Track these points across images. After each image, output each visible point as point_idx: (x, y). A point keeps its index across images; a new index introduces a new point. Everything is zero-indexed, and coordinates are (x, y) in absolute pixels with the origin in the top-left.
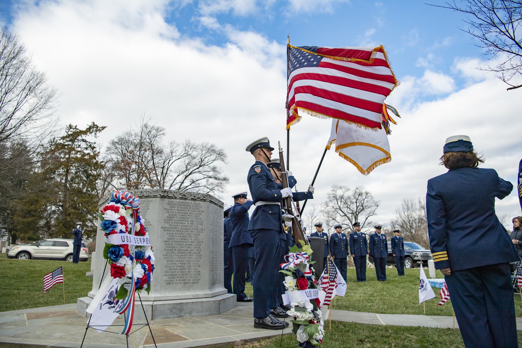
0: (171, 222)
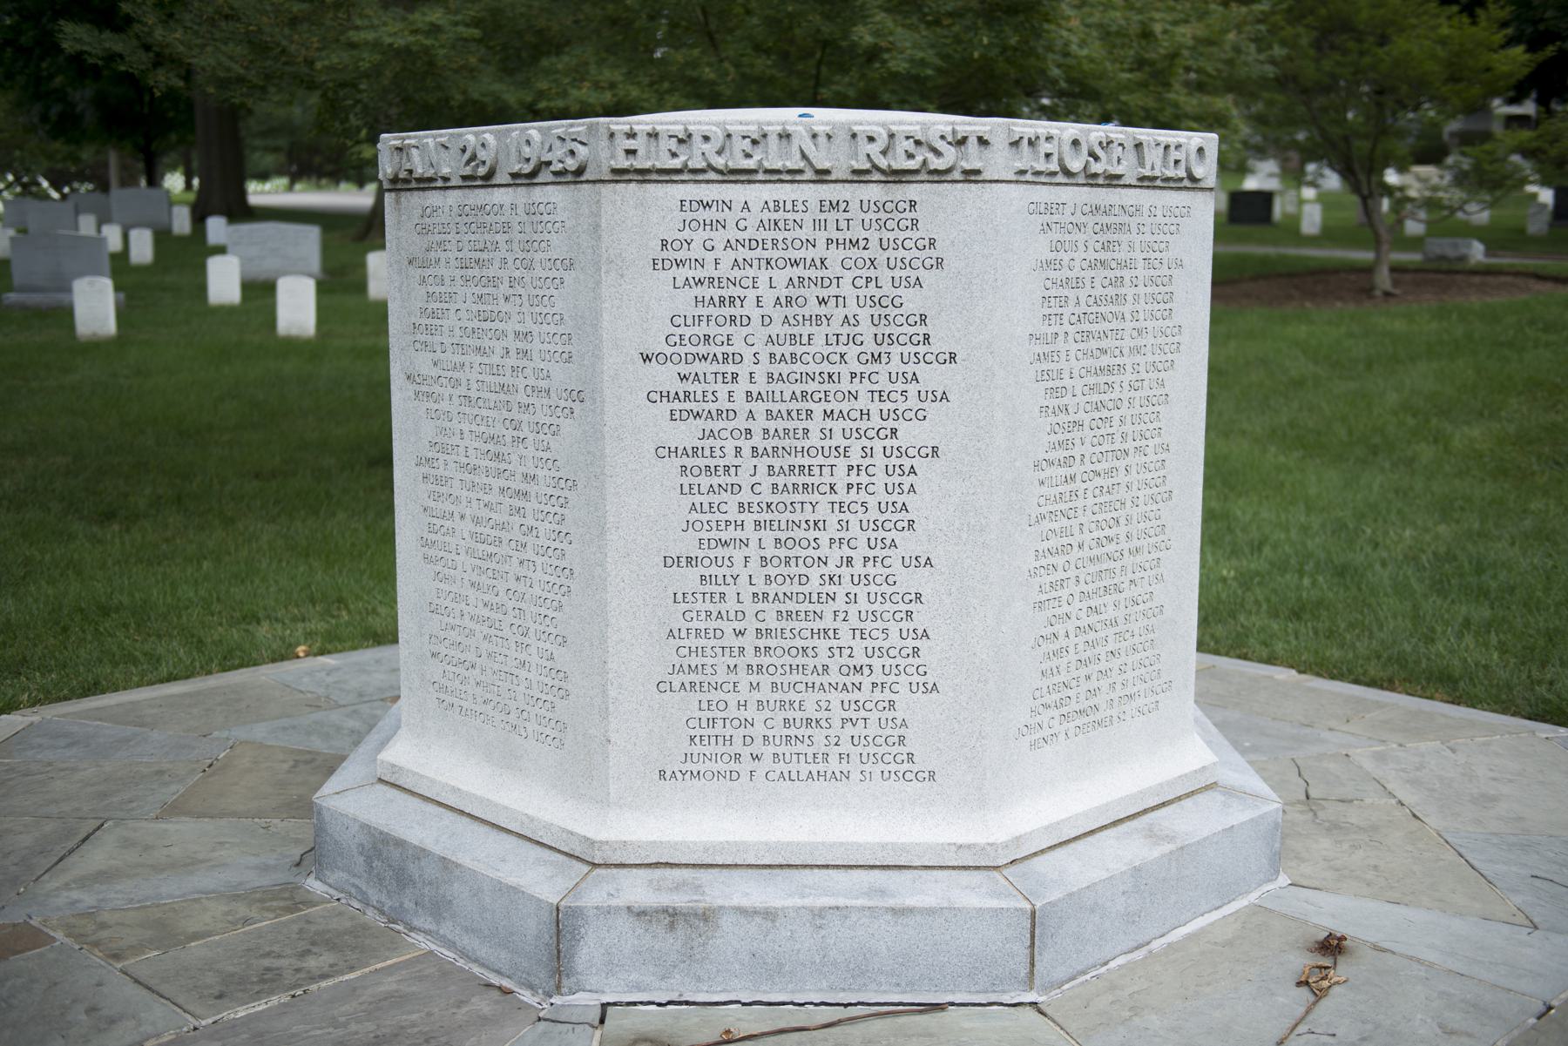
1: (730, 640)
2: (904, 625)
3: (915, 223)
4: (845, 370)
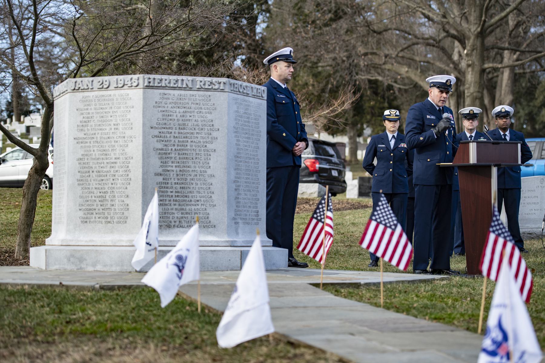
0: (86, 128)
1: (169, 194)
2: (209, 191)
3: (210, 100)
4: (195, 131)
